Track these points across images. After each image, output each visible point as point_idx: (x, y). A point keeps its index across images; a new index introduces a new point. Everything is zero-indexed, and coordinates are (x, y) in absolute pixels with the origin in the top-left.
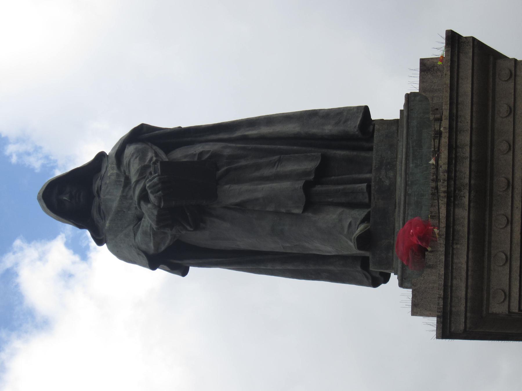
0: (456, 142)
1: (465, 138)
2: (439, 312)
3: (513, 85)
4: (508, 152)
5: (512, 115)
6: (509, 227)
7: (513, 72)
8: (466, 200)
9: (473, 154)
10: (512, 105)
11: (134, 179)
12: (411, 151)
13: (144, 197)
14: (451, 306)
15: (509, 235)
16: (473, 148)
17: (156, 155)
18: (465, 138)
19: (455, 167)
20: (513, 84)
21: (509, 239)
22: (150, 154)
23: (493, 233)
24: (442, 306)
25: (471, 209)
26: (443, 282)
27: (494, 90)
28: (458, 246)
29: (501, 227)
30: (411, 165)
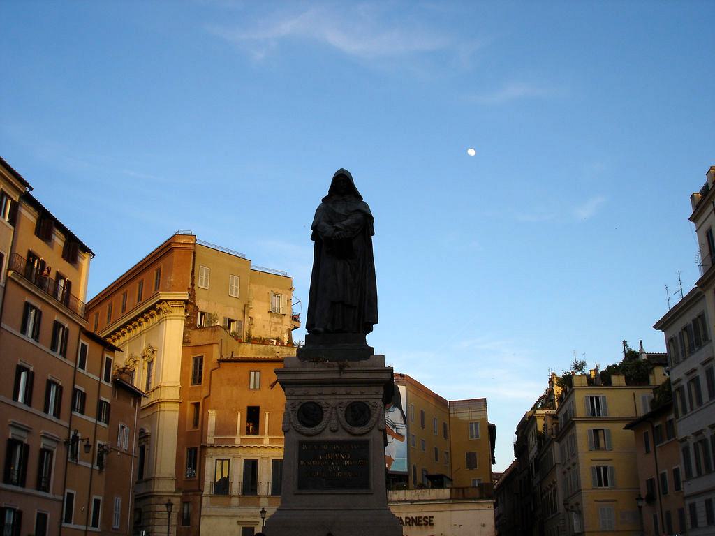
11: (344, 223)
13: (337, 229)
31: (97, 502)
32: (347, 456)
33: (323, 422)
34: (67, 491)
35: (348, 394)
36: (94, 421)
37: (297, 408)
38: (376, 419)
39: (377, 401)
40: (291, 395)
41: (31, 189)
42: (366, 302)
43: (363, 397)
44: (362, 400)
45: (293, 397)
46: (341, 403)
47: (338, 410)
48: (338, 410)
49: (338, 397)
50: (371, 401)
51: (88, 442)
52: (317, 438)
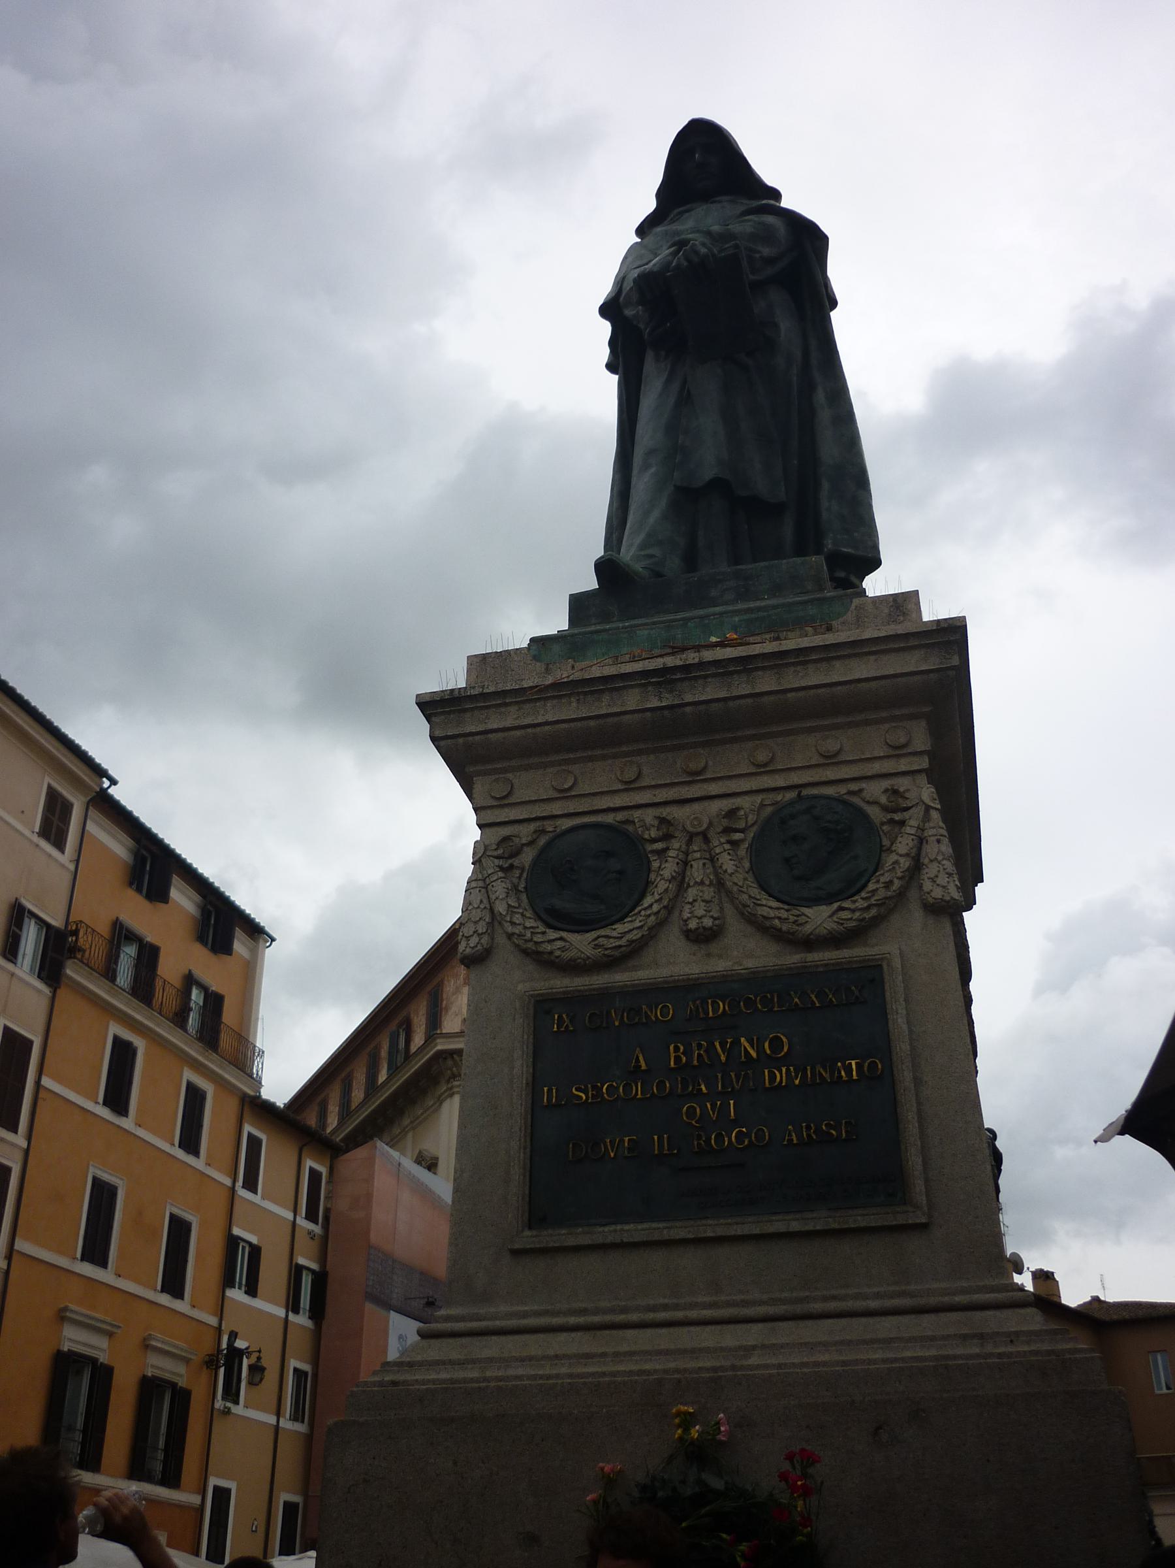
0: (757, 669)
1: (766, 683)
2: (459, 692)
3: (878, 755)
4: (753, 764)
5: (822, 761)
6: (620, 787)
7: (904, 751)
8: (655, 703)
9: (738, 702)
10: (842, 757)
12: (761, 614)
14: (472, 709)
15: (606, 789)
16: (750, 701)
17: (770, 261)
18: (766, 683)
19: (714, 675)
20: (882, 755)
21: (598, 791)
22: (766, 251)
23: (610, 762)
24: (469, 694)
25: (640, 715)
26: (509, 689)
27: (867, 723)
28: (574, 704)
29: (618, 775)
30: (737, 619)
31: (290, 1508)
32: (776, 1043)
33: (647, 901)
34: (213, 1481)
35: (763, 769)
36: (281, 1312)
37: (527, 857)
38: (905, 863)
39: (903, 784)
40: (503, 802)
41: (113, 782)
42: (826, 485)
43: (831, 774)
44: (830, 791)
45: (514, 814)
46: (732, 813)
47: (718, 843)
48: (718, 843)
49: (714, 789)
50: (875, 790)
51: (259, 1358)
52: (620, 978)
